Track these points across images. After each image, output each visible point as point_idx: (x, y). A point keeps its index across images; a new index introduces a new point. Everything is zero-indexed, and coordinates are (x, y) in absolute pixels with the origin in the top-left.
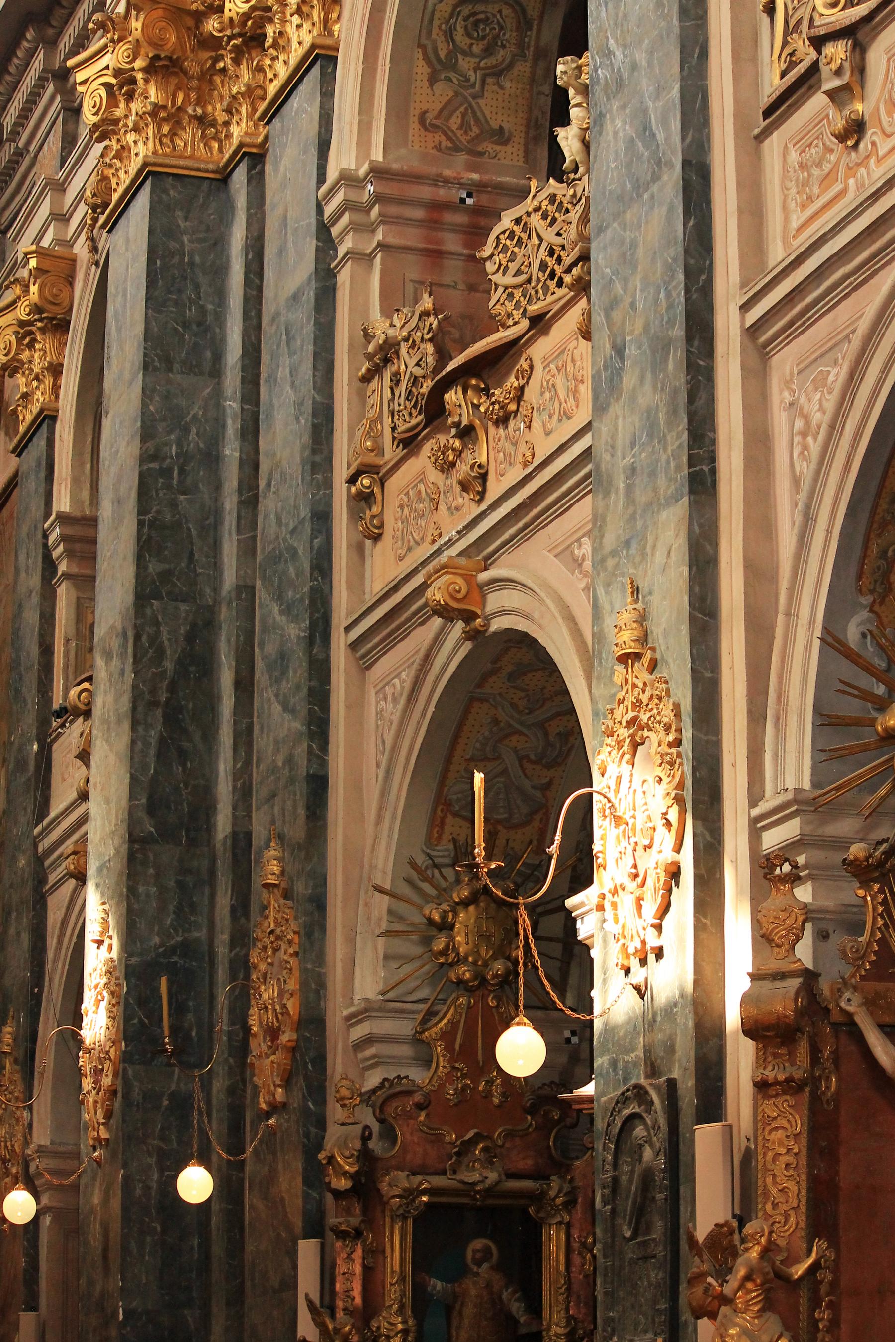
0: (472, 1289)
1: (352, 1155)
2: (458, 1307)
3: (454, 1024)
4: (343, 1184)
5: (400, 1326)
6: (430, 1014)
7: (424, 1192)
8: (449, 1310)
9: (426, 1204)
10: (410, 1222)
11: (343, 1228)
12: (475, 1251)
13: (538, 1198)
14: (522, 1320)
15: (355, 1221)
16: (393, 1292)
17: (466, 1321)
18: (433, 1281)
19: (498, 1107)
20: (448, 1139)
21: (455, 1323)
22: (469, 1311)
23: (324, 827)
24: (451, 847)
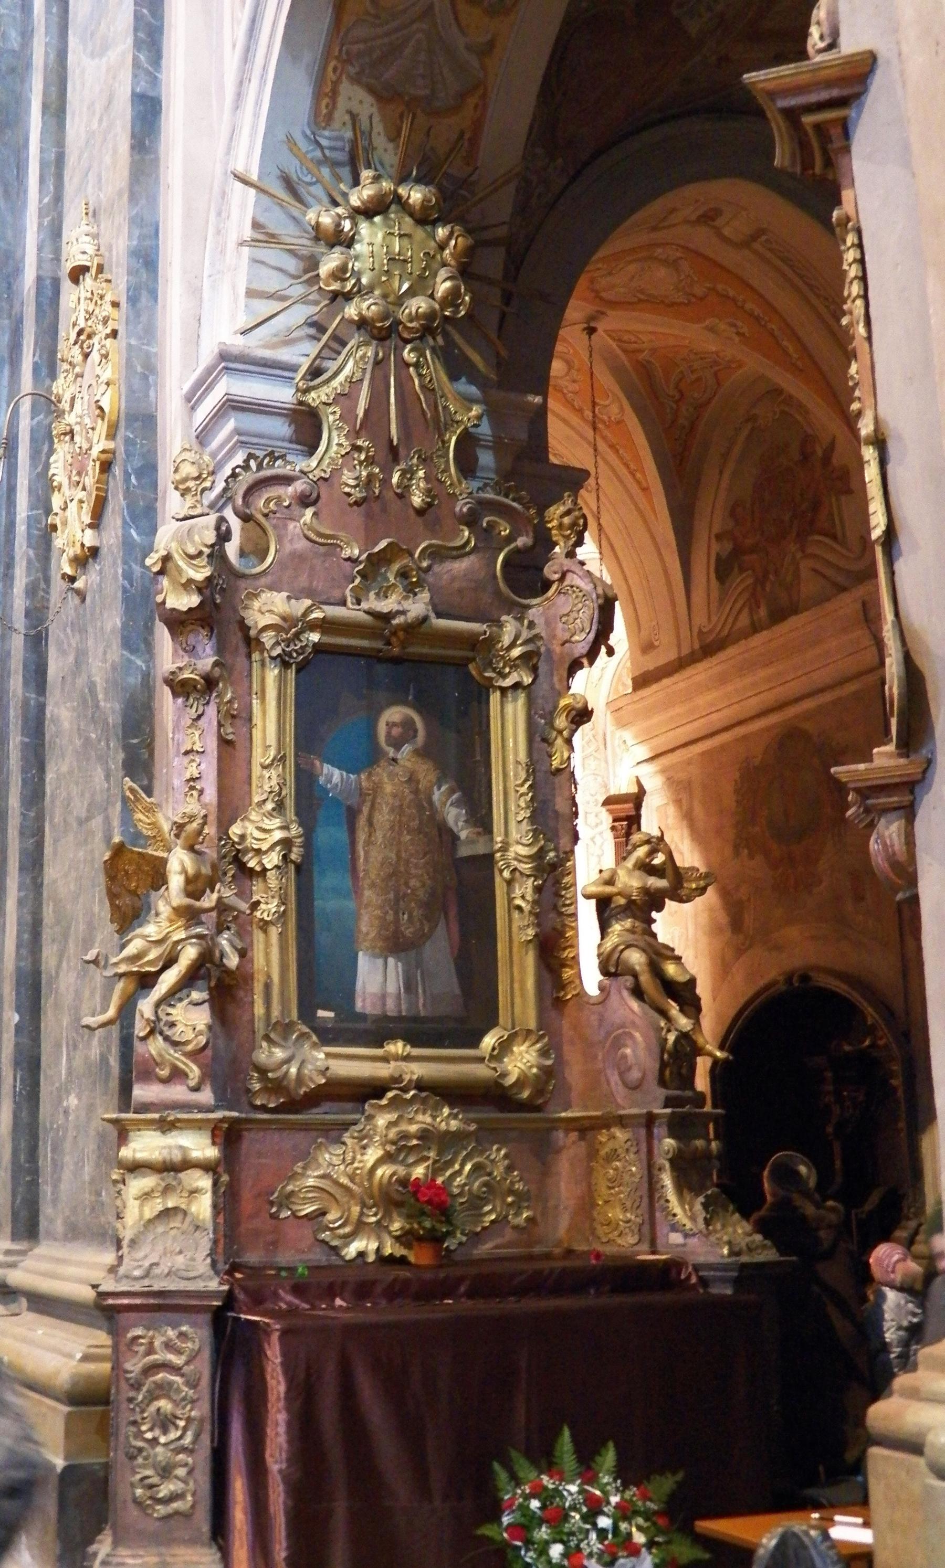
0: (388, 782)
1: (200, 553)
2: (365, 810)
3: (354, 383)
4: (188, 601)
5: (278, 835)
6: (315, 372)
7: (313, 626)
8: (352, 815)
9: (318, 648)
10: (291, 674)
11: (186, 675)
12: (390, 725)
13: (482, 647)
14: (463, 835)
15: (207, 661)
16: (267, 779)
17: (379, 836)
18: (327, 768)
19: (420, 512)
20: (347, 553)
21: (362, 836)
22: (383, 817)
23: (156, 162)
24: (349, 134)
